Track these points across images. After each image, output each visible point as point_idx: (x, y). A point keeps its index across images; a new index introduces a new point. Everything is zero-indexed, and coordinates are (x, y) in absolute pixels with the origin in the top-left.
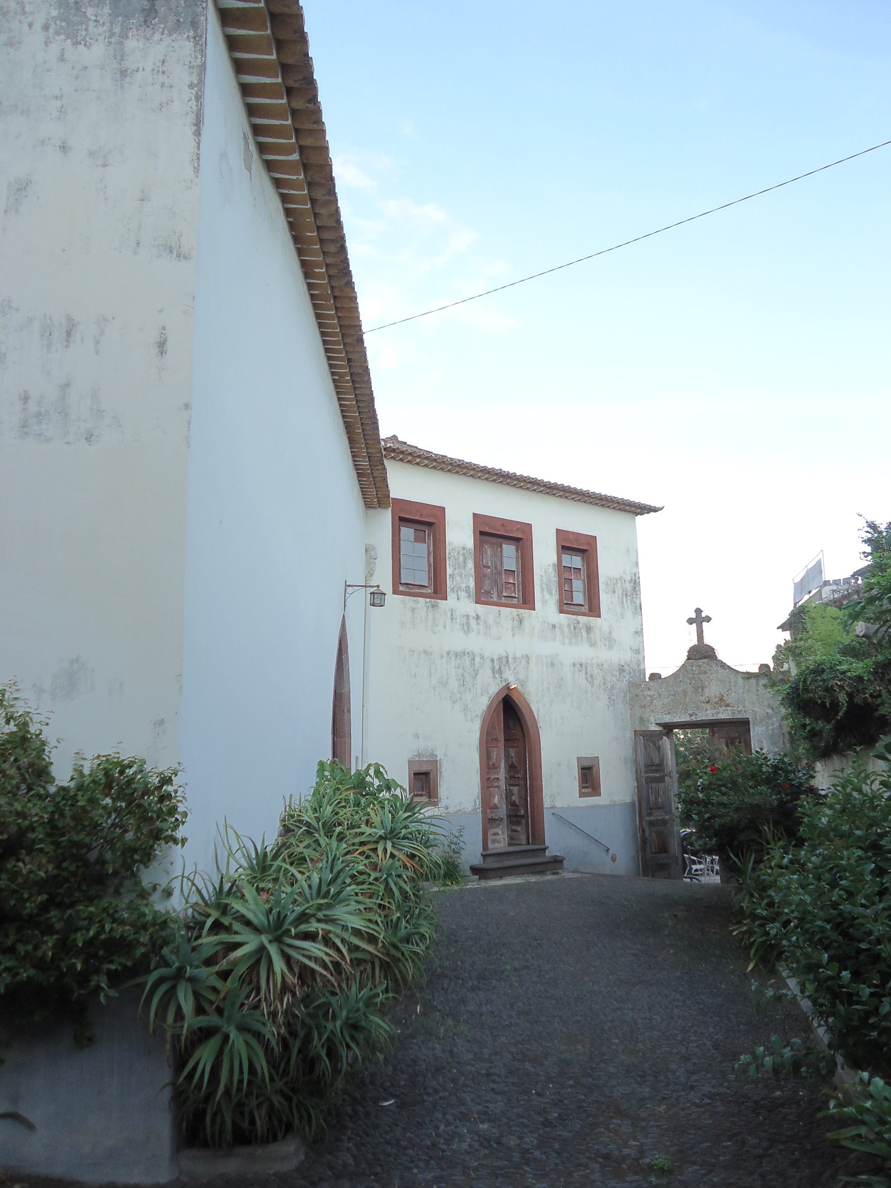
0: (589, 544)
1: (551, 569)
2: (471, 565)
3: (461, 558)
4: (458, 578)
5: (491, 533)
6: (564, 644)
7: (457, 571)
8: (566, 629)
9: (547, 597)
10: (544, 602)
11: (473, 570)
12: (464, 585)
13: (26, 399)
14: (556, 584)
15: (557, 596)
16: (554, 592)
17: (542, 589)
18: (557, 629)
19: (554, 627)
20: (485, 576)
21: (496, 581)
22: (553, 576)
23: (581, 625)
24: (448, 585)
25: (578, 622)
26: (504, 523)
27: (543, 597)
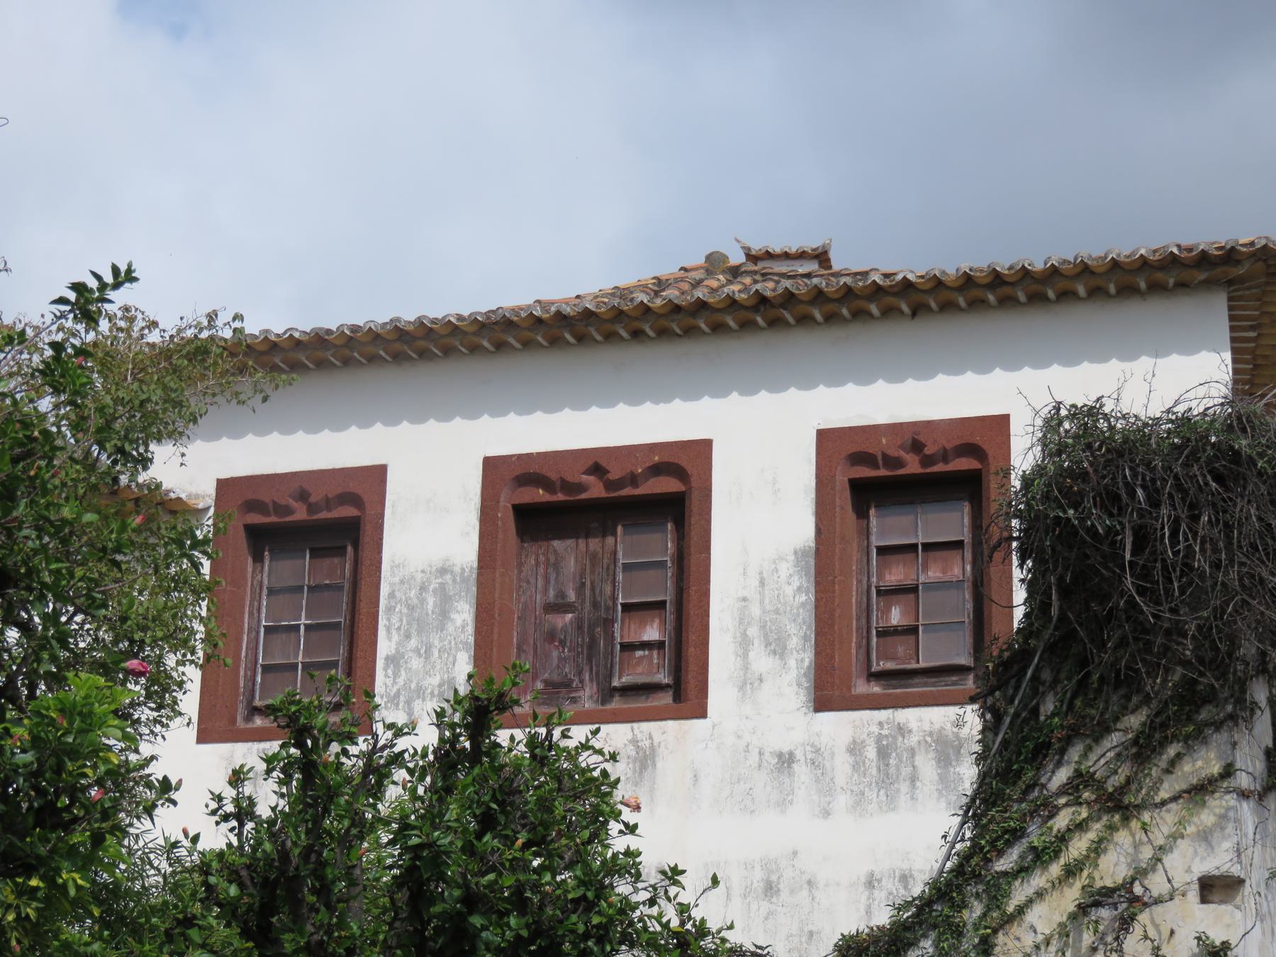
1: (786, 568)
2: (464, 615)
3: (431, 601)
4: (416, 663)
5: (537, 508)
6: (826, 813)
7: (413, 643)
8: (841, 766)
9: (761, 661)
10: (748, 683)
11: (470, 629)
12: (435, 681)
14: (807, 615)
15: (808, 657)
16: (794, 642)
17: (744, 644)
18: (801, 769)
19: (786, 761)
20: (551, 636)
21: (593, 644)
22: (794, 593)
23: (913, 740)
24: (379, 687)
25: (902, 730)
27: (746, 668)
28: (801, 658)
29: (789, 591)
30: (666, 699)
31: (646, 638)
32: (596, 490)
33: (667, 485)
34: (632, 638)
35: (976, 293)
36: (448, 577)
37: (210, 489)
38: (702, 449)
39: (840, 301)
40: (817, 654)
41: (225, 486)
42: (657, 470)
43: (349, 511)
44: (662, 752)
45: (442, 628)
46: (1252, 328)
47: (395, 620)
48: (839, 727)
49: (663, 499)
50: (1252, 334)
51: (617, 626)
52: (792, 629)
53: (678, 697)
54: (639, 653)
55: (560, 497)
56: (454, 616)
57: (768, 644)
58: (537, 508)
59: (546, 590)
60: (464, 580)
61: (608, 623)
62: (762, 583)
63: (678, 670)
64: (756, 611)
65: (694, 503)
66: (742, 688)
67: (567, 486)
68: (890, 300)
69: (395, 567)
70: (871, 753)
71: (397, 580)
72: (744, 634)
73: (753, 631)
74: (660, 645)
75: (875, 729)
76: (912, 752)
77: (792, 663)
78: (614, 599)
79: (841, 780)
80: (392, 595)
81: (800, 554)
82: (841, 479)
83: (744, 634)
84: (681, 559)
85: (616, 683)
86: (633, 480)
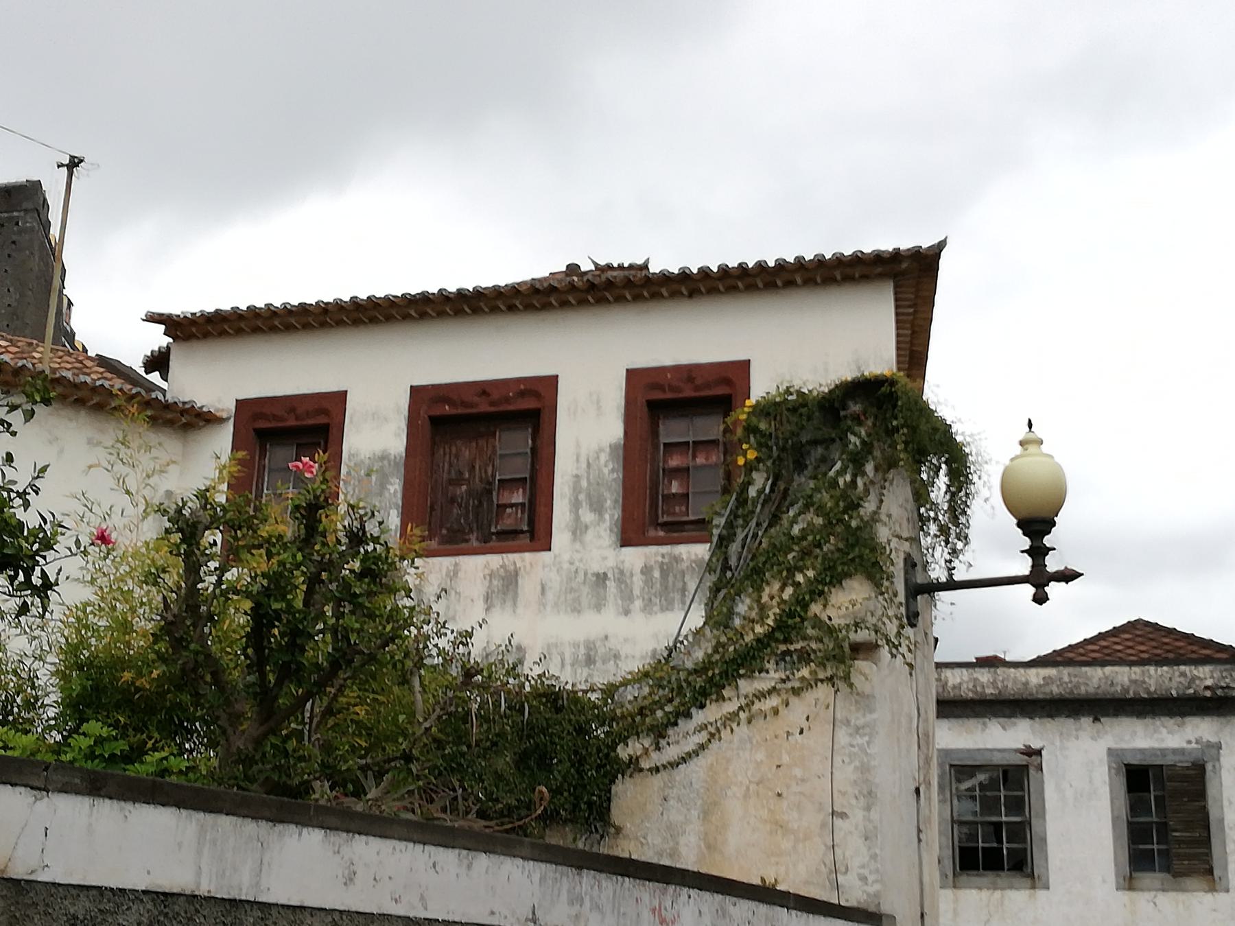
0: (728, 382)
1: (604, 457)
5: (444, 418)
6: (627, 612)
8: (638, 582)
9: (587, 516)
10: (578, 530)
11: (399, 495)
13: (938, 386)
15: (617, 514)
17: (576, 505)
18: (611, 585)
19: (602, 578)
20: (453, 500)
22: (610, 472)
25: (677, 559)
26: (483, 389)
28: (613, 513)
29: (606, 471)
30: (525, 540)
31: (513, 501)
32: (485, 408)
33: (529, 404)
34: (503, 501)
35: (730, 282)
36: (386, 462)
37: (232, 407)
38: (551, 382)
39: (643, 286)
40: (624, 511)
41: (240, 403)
42: (522, 394)
43: (322, 420)
44: (522, 572)
45: (381, 494)
46: (910, 307)
47: (350, 489)
48: (635, 557)
49: (526, 410)
50: (911, 310)
51: (494, 494)
52: (607, 495)
53: (532, 538)
54: (509, 510)
55: (460, 411)
56: (389, 487)
57: (591, 505)
58: (444, 418)
59: (449, 473)
60: (396, 464)
61: (490, 492)
62: (589, 465)
63: (531, 522)
64: (584, 484)
65: (545, 416)
66: (574, 533)
67: (464, 404)
68: (675, 287)
69: (351, 456)
70: (657, 574)
71: (352, 464)
72: (577, 499)
73: (582, 497)
74: (523, 505)
75: (660, 559)
76: (683, 574)
77: (607, 517)
78: (494, 476)
79: (637, 592)
80: (349, 473)
81: (613, 448)
82: (641, 401)
83: (577, 499)
84: (534, 450)
85: (493, 530)
86: (507, 400)
